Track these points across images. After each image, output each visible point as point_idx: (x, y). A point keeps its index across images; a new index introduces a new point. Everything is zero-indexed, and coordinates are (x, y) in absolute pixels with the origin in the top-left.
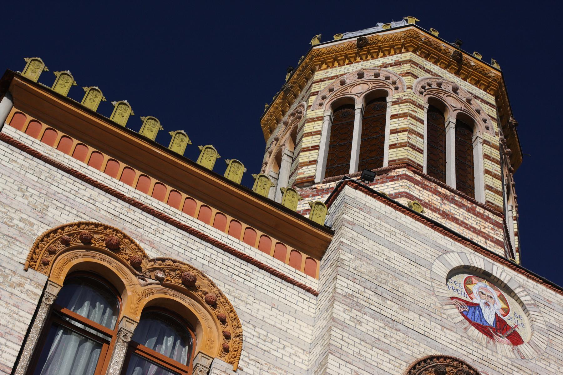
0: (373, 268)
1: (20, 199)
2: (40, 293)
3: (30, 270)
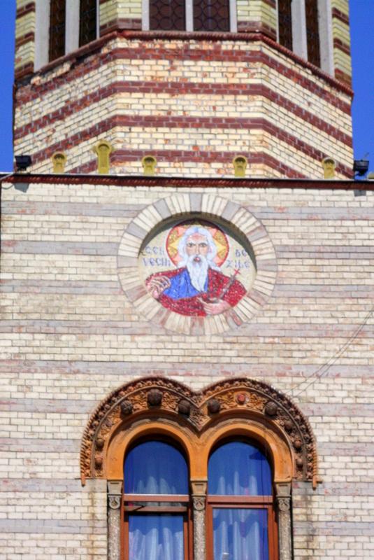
0: (41, 297)
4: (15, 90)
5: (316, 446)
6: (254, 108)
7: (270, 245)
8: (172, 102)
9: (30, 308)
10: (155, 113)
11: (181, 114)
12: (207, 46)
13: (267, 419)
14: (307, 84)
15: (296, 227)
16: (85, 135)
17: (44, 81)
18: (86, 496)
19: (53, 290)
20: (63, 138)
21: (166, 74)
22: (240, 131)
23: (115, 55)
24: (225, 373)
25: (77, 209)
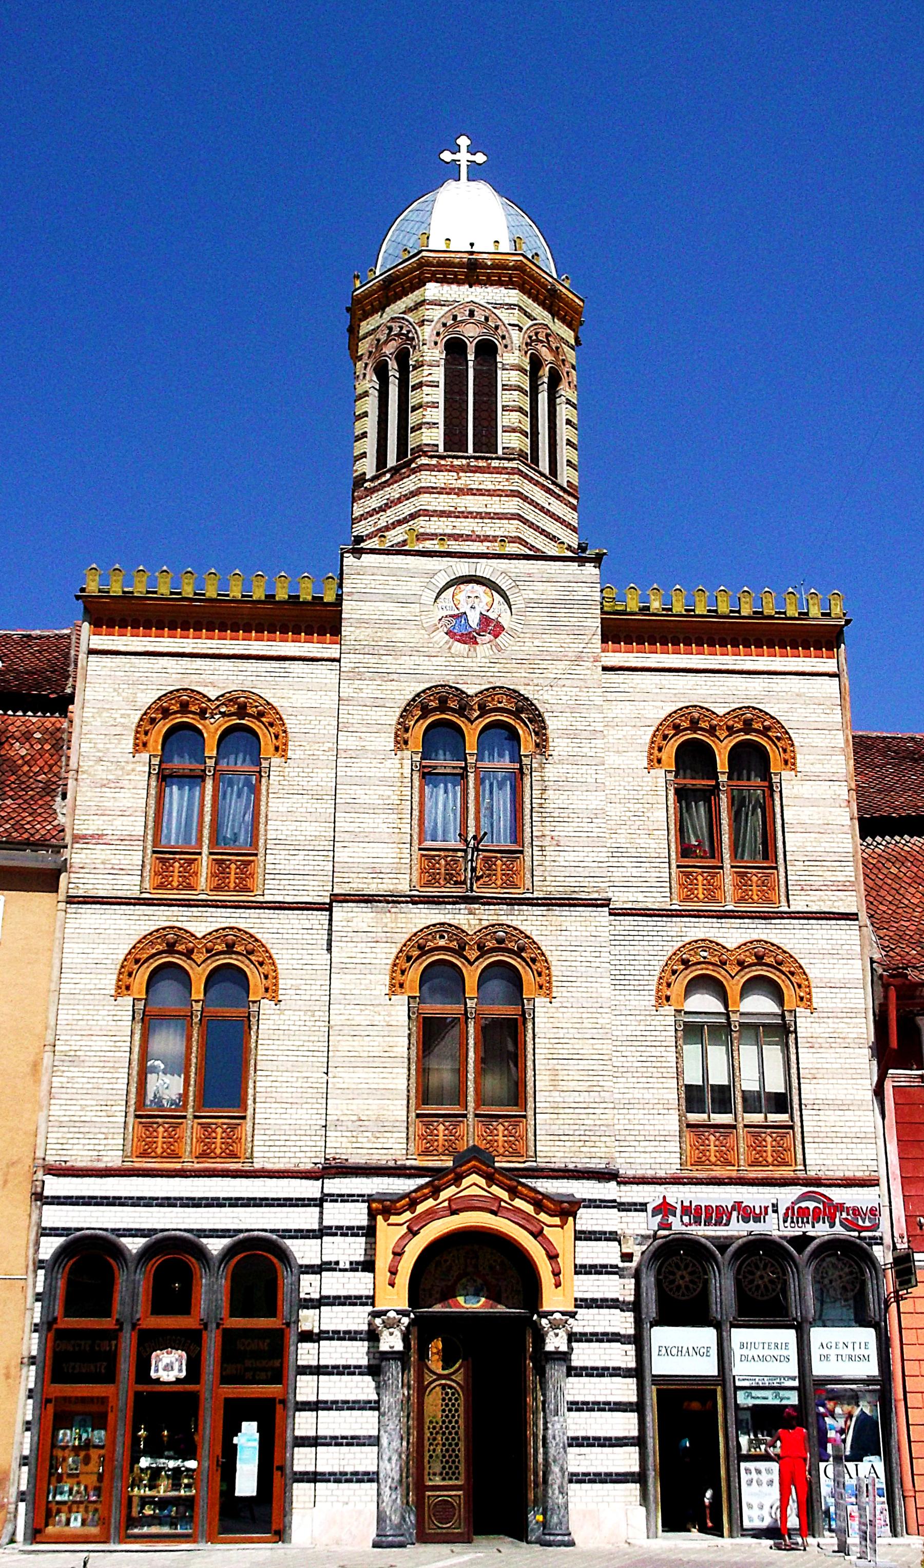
1: (116, 698)
2: (147, 769)
3: (137, 755)
4: (353, 491)
5: (548, 732)
6: (512, 505)
7: (521, 598)
8: (458, 501)
9: (361, 637)
10: (446, 508)
11: (463, 509)
12: (482, 463)
13: (516, 714)
14: (548, 491)
15: (540, 587)
16: (400, 523)
17: (372, 485)
18: (398, 761)
19: (377, 626)
20: (385, 524)
21: (454, 482)
22: (502, 521)
23: (421, 468)
24: (490, 682)
25: (394, 573)
